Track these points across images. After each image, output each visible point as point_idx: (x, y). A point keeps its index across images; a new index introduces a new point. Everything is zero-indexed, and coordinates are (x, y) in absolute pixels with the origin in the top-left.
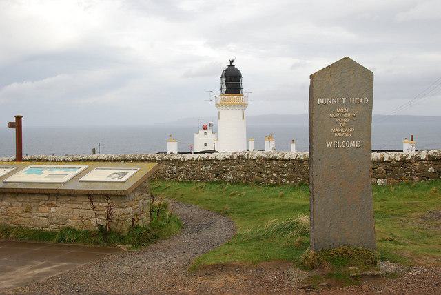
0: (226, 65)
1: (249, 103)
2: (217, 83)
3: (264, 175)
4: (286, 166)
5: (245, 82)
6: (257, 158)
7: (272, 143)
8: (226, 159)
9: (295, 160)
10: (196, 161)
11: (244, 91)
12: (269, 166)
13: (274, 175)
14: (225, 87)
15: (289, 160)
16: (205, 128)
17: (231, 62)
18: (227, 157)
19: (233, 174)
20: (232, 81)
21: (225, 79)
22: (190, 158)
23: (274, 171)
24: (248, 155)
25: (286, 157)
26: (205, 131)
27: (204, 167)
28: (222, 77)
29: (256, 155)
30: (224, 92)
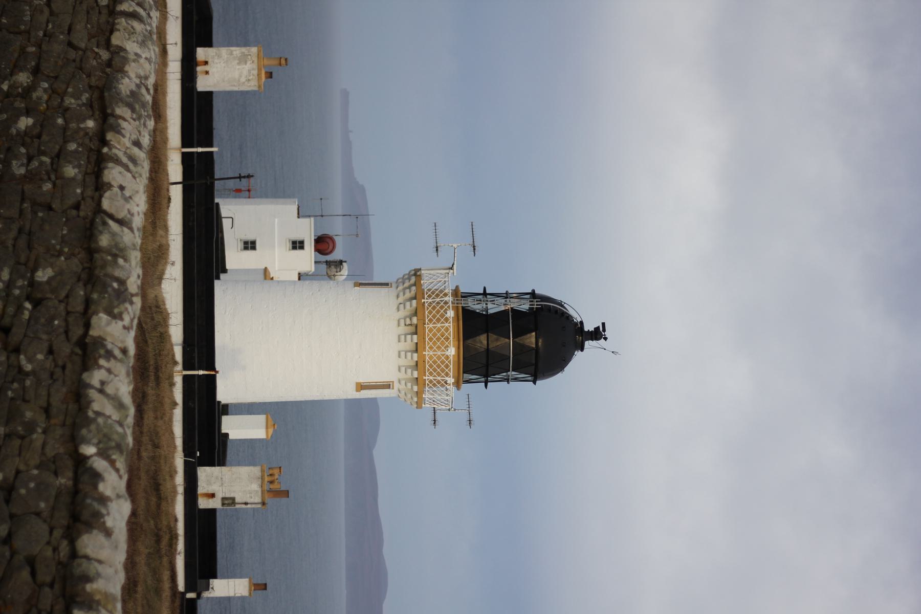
2: (512, 277)
3: (23, 78)
5: (512, 394)
9: (98, 210)
11: (476, 389)
12: (70, 101)
13: (25, 122)
14: (493, 309)
15: (101, 187)
16: (323, 244)
17: (597, 334)
20: (522, 339)
21: (525, 306)
23: (43, 123)
24: (134, 16)
25: (113, 174)
26: (310, 246)
28: (533, 294)
29: (132, 47)
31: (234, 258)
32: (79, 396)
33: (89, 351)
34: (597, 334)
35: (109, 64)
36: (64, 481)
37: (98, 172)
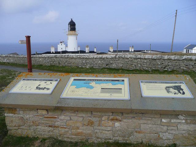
0: (70, 20)
1: (78, 34)
2: (67, 27)
4: (146, 61)
5: (77, 27)
6: (130, 57)
7: (88, 48)
8: (112, 58)
10: (96, 58)
14: (70, 28)
16: (61, 43)
17: (72, 19)
18: (113, 57)
19: (116, 65)
20: (72, 26)
22: (92, 57)
26: (62, 44)
27: (100, 61)
28: (68, 25)
29: (129, 56)
30: (70, 30)
31: (64, 50)
32: (174, 60)
33: (169, 59)
34: (72, 19)
35: (131, 58)
36: (185, 61)
37: (146, 59)
